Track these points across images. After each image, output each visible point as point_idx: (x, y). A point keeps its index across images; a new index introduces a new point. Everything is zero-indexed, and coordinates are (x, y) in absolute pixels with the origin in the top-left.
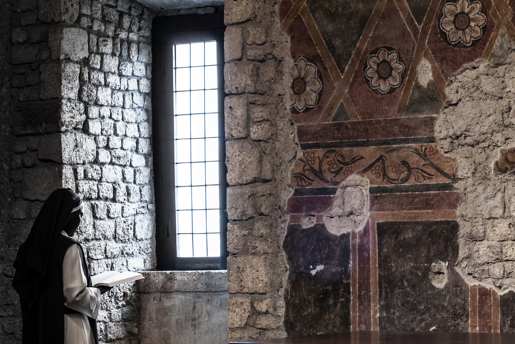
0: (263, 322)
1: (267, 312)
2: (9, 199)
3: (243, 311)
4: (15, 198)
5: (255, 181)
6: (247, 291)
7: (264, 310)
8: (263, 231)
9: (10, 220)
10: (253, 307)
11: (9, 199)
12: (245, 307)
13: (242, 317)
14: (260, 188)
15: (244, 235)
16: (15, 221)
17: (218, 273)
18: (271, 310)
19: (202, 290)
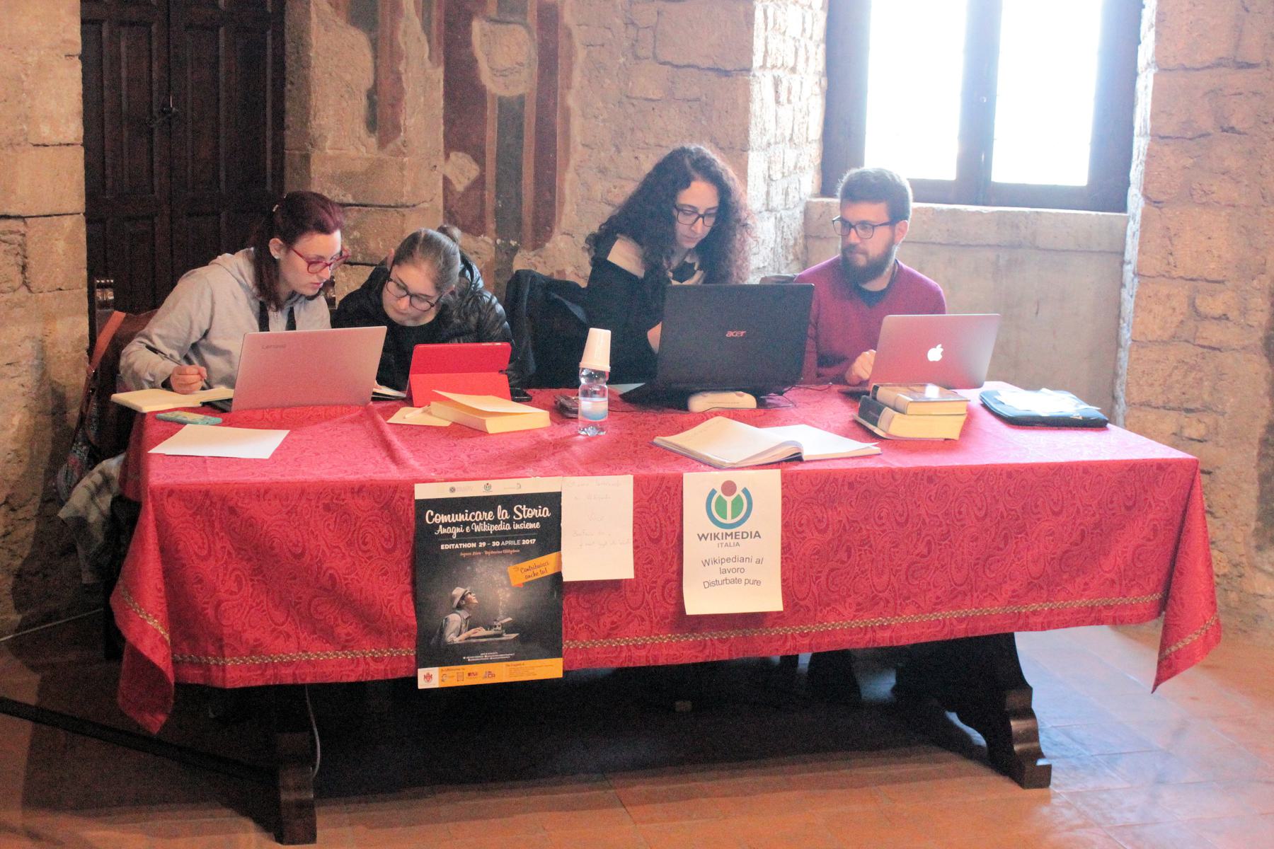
0: (1213, 333)
1: (1224, 317)
2: (622, 60)
3: (1170, 311)
4: (637, 57)
5: (1219, 64)
6: (1182, 274)
7: (1218, 312)
8: (1232, 163)
9: (625, 100)
10: (1193, 305)
11: (622, 60)
12: (1174, 303)
13: (1166, 322)
14: (1239, 79)
15: (1185, 167)
16: (635, 102)
17: (974, 213)
18: (1233, 315)
19: (939, 240)
